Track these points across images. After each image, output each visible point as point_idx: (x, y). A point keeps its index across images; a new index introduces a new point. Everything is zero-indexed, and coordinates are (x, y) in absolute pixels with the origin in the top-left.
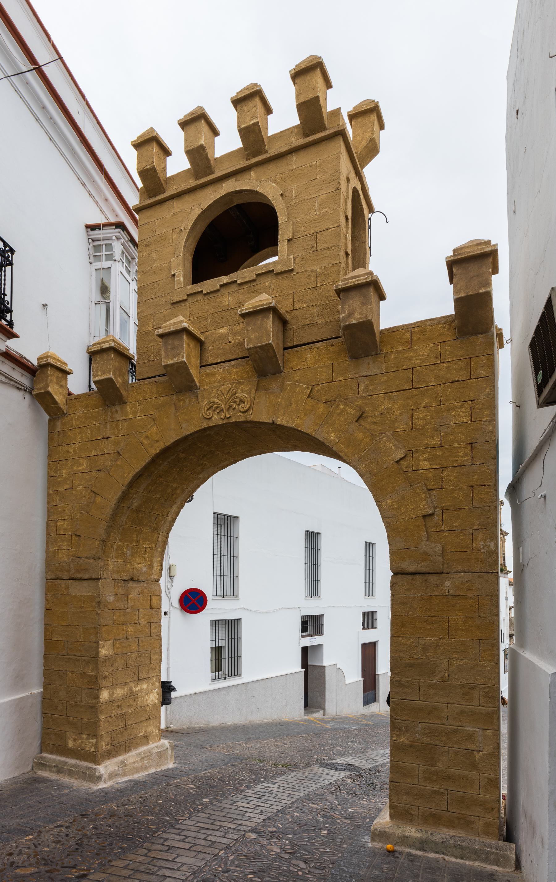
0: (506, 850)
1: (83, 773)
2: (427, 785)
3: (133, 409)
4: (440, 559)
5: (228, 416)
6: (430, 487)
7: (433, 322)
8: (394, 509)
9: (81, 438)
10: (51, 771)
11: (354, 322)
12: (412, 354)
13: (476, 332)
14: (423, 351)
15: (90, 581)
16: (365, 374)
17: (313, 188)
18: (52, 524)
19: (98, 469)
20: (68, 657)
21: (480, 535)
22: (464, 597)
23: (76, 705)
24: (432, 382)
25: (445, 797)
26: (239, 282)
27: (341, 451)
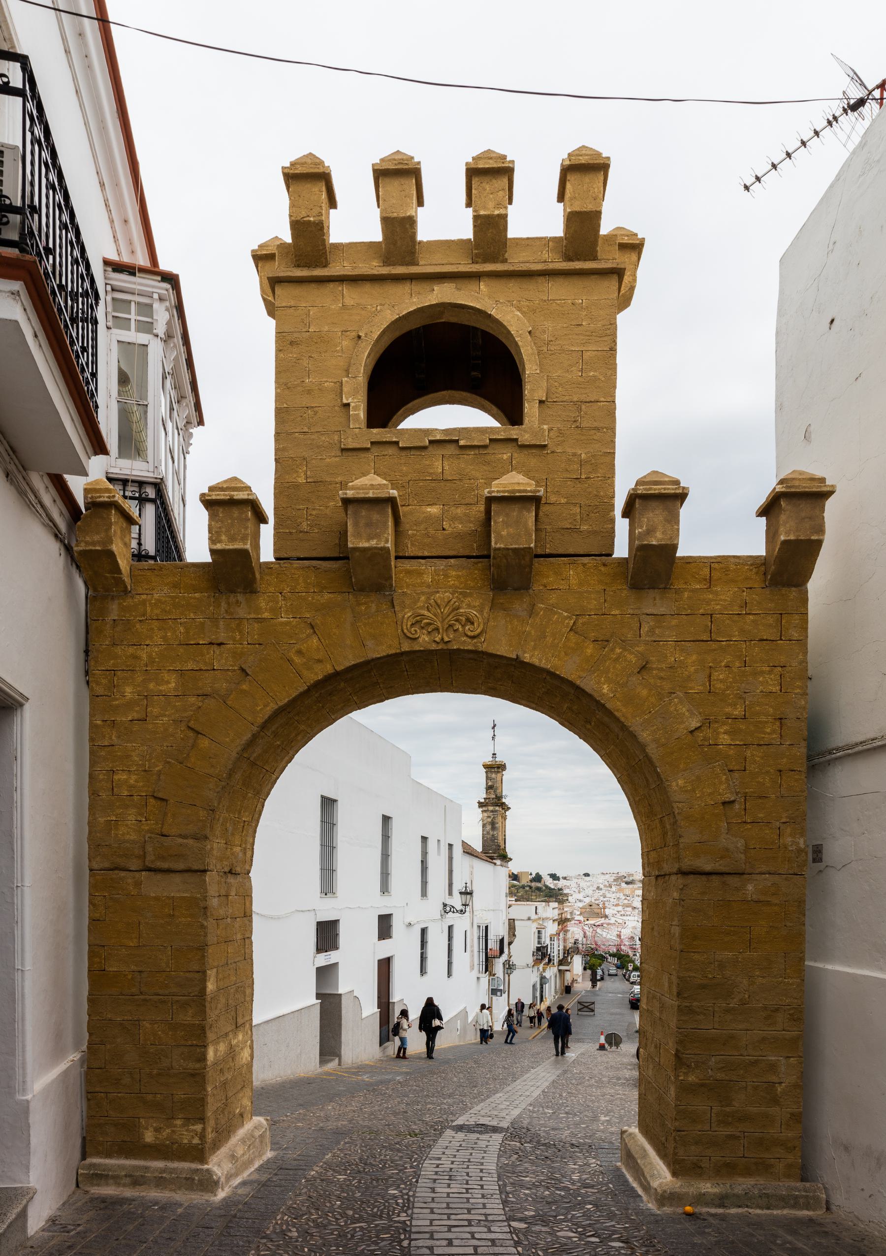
0: (815, 1191)
1: (186, 1179)
2: (721, 1129)
3: (271, 604)
4: (742, 856)
5: (446, 639)
6: (731, 768)
7: (737, 561)
8: (686, 791)
9: (164, 638)
10: (118, 1184)
11: (654, 543)
12: (711, 596)
13: (790, 584)
14: (724, 596)
15: (186, 875)
16: (649, 611)
17: (577, 337)
18: (101, 777)
19: (200, 692)
20: (142, 997)
21: (789, 830)
22: (768, 903)
23: (159, 1074)
24: (735, 636)
25: (742, 1141)
26: (462, 443)
27: (618, 710)
